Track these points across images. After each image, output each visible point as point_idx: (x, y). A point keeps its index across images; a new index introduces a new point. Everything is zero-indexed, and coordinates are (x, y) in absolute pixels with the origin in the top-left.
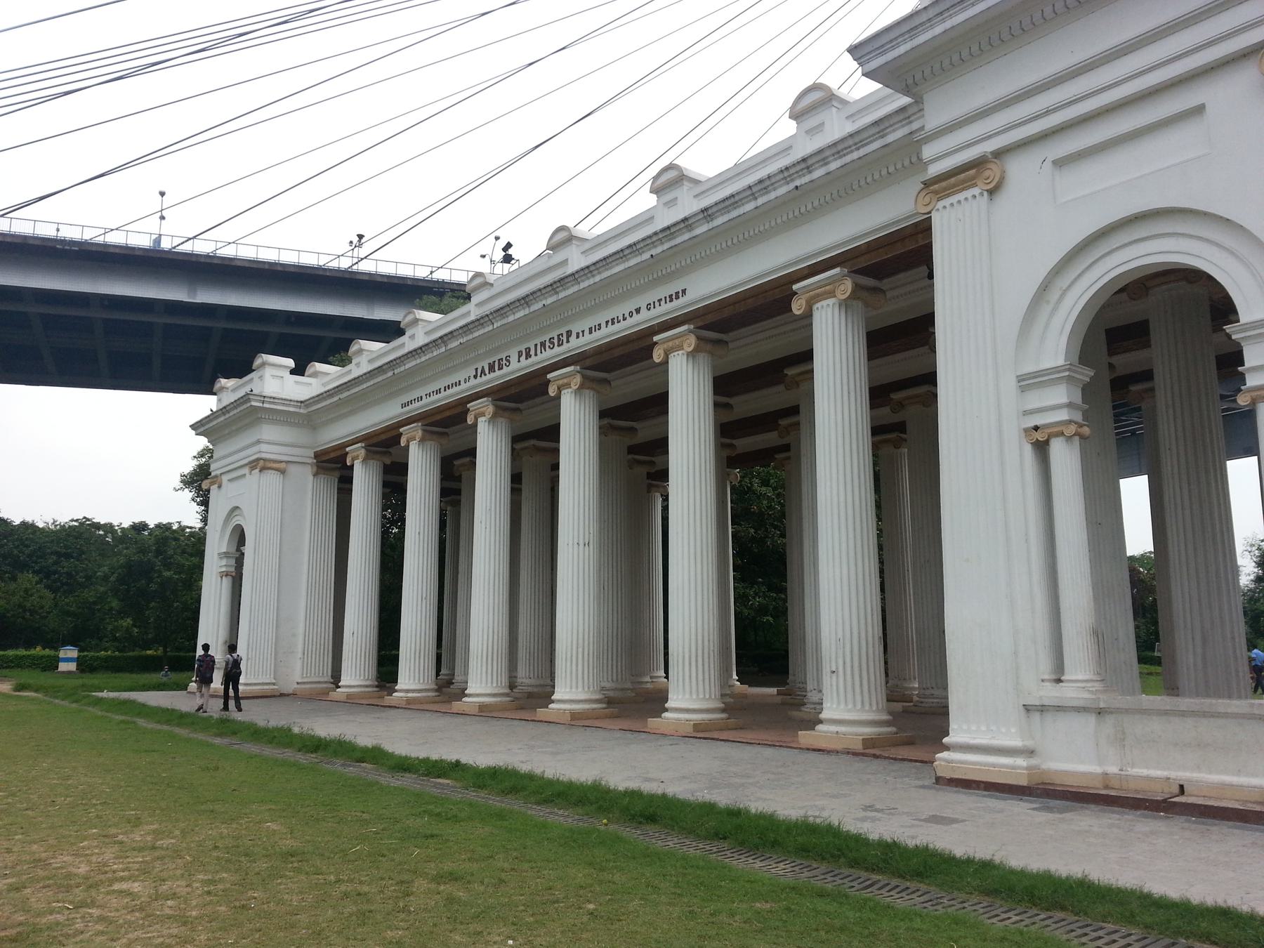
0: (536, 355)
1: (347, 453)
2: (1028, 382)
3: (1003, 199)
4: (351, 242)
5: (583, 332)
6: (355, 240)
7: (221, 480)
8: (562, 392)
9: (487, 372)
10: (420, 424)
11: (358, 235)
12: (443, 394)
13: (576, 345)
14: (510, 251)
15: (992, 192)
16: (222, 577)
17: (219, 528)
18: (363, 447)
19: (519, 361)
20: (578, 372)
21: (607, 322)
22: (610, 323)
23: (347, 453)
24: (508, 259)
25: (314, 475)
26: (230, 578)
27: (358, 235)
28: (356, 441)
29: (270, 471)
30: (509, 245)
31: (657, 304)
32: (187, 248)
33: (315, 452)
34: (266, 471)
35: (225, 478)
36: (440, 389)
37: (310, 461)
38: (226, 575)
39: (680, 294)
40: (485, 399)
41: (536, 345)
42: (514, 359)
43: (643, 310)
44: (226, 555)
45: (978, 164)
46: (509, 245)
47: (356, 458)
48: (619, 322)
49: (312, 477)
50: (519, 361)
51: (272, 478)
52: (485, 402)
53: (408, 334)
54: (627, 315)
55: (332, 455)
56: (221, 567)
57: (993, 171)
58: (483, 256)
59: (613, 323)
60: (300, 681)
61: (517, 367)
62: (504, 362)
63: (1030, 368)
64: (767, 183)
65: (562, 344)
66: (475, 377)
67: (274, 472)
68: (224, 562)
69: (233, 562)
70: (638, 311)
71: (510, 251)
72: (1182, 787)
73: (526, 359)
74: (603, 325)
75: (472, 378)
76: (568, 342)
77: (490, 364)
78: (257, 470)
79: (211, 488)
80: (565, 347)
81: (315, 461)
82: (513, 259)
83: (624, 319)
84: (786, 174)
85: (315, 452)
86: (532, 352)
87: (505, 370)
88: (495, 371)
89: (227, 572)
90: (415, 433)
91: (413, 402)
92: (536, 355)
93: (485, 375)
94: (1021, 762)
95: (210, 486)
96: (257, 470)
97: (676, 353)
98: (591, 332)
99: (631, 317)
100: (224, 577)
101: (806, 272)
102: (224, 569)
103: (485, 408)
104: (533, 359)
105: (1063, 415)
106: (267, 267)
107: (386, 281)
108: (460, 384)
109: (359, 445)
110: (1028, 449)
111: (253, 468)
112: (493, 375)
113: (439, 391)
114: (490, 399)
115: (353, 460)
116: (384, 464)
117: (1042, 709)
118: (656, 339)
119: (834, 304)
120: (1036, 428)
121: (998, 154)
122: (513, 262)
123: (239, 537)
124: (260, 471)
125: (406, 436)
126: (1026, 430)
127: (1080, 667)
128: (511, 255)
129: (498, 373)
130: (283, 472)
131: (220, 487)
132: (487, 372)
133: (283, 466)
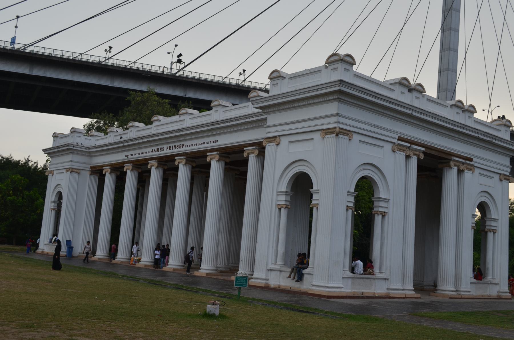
0: (172, 149)
1: (103, 169)
2: (279, 194)
3: (279, 146)
4: (106, 50)
5: (187, 145)
6: (108, 49)
7: (53, 172)
8: (180, 164)
9: (156, 151)
10: (131, 164)
11: (109, 47)
12: (140, 155)
13: (184, 149)
14: (181, 58)
15: (277, 145)
16: (52, 210)
17: (52, 191)
18: (110, 168)
19: (167, 150)
20: (185, 159)
22: (196, 145)
23: (103, 169)
24: (179, 61)
25: (90, 175)
26: (55, 211)
27: (109, 47)
28: (107, 165)
29: (74, 173)
30: (180, 55)
31: (210, 142)
32: (30, 49)
33: (91, 166)
34: (73, 173)
35: (55, 172)
36: (139, 153)
37: (89, 169)
38: (54, 210)
39: (216, 141)
40: (155, 161)
41: (173, 146)
42: (165, 149)
43: (206, 143)
44: (54, 202)
45: (275, 137)
46: (180, 55)
47: (107, 171)
48: (198, 145)
49: (89, 176)
50: (167, 150)
51: (75, 175)
52: (154, 162)
53: (130, 129)
54: (201, 144)
55: (98, 169)
56: (52, 206)
57: (278, 139)
58: (169, 53)
59: (197, 145)
60: (80, 252)
61: (166, 152)
62: (162, 149)
63: (280, 190)
64: (239, 118)
65: (181, 148)
66: (152, 152)
67: (75, 173)
68: (53, 204)
69: (56, 205)
70: (204, 143)
71: (181, 58)
72: (291, 288)
73: (169, 150)
74: (194, 145)
75: (151, 152)
77: (157, 149)
78: (69, 172)
79: (49, 175)
80: (182, 149)
81: (91, 170)
82: (182, 62)
83: (200, 145)
84: (243, 117)
85: (91, 166)
86: (171, 148)
87: (162, 152)
88: (159, 151)
89: (54, 208)
90: (130, 167)
91: (130, 155)
92: (172, 149)
93: (155, 152)
94: (264, 282)
95: (49, 174)
96: (69, 172)
97: (213, 160)
98: (190, 146)
99: (202, 144)
100: (53, 211)
101: (248, 145)
102: (53, 207)
103: (154, 164)
104: (171, 151)
105: (283, 203)
106: (66, 61)
107: (121, 69)
108: (146, 153)
109: (108, 167)
110: (277, 209)
111: (67, 171)
113: (139, 154)
114: (156, 161)
115: (106, 172)
116: (117, 175)
117: (271, 270)
118: (208, 154)
119: (254, 156)
120: (279, 205)
121: (279, 136)
122: (182, 63)
123: (60, 196)
124: (70, 173)
125: (126, 167)
126: (277, 205)
127: (280, 262)
128: (181, 60)
129: (160, 153)
130: (79, 173)
131: (53, 175)
132: (156, 151)
133: (79, 171)
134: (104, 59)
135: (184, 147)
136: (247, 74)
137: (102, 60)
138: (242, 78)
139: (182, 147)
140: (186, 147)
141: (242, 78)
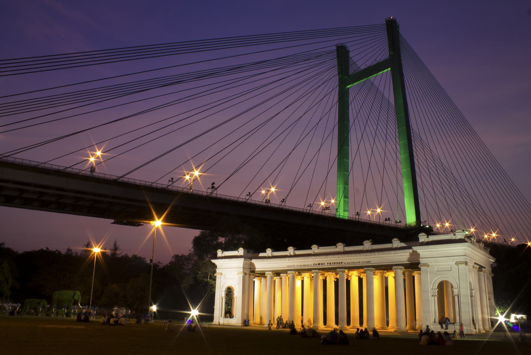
14: (214, 185)
24: (213, 187)
30: (213, 183)
42: (326, 264)
46: (213, 183)
66: (314, 265)
71: (214, 185)
74: (351, 263)
76: (342, 264)
80: (341, 264)
92: (333, 264)
93: (317, 265)
112: (319, 266)
134: (167, 186)
135: (343, 264)
136: (251, 194)
137: (165, 187)
138: (248, 197)
139: (341, 263)
140: (344, 263)
141: (248, 197)
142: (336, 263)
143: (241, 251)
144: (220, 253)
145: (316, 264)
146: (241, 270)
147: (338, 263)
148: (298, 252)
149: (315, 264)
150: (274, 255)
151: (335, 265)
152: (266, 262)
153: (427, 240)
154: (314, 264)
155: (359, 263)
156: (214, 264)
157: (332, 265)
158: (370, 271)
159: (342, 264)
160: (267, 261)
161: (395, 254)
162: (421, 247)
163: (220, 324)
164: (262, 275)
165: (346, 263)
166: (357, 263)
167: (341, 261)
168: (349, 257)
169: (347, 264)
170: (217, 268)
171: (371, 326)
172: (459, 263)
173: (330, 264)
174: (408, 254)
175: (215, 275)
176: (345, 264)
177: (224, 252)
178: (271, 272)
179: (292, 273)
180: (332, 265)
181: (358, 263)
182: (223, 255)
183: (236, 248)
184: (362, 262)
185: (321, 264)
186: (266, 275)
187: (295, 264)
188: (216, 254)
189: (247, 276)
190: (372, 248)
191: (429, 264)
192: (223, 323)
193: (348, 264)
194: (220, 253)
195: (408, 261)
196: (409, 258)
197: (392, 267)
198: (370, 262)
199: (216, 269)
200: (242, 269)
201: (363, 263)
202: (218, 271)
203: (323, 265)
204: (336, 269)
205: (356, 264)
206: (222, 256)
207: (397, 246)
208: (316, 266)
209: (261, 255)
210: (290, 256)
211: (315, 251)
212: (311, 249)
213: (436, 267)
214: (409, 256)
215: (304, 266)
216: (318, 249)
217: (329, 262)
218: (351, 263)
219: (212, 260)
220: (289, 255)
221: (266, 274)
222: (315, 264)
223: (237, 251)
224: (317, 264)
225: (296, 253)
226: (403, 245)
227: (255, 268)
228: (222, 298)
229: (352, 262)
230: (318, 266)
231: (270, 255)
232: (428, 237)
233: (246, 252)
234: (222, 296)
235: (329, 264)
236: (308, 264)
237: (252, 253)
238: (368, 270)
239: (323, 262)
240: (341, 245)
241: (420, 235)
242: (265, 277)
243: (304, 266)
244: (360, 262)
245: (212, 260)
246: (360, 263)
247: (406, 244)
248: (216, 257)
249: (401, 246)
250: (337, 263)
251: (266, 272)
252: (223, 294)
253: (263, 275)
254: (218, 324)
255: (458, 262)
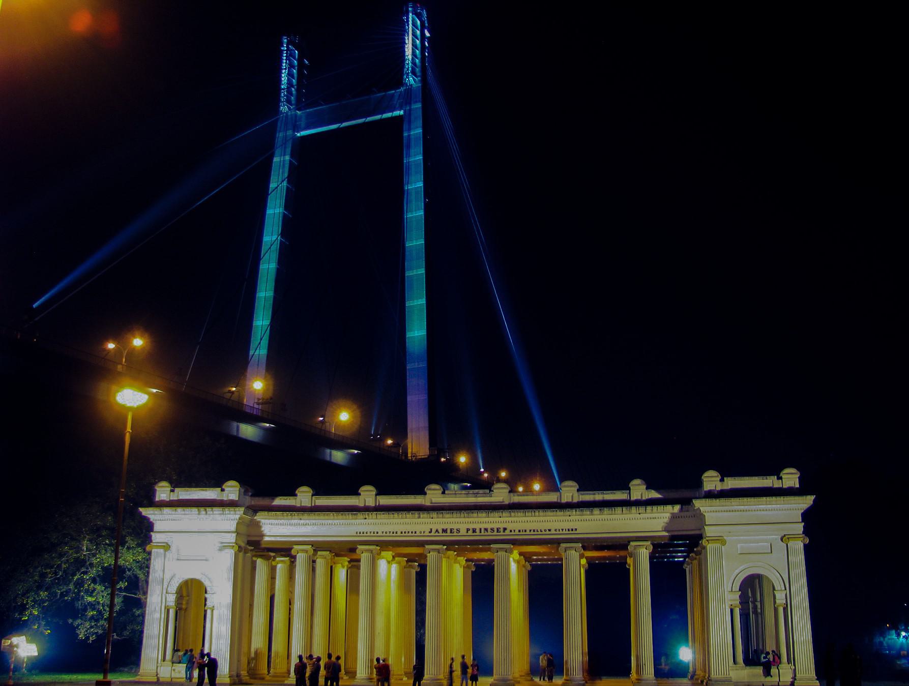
0: (481, 532)
19: (467, 532)
21: (530, 531)
42: (463, 532)
50: (467, 532)
73: (473, 532)
74: (528, 531)
76: (504, 532)
92: (481, 532)
93: (438, 533)
112: (444, 534)
135: (507, 532)
140: (511, 531)
142: (489, 530)
143: (232, 490)
144: (163, 492)
145: (437, 531)
146: (232, 538)
147: (495, 530)
148: (385, 500)
149: (434, 531)
150: (316, 504)
151: (486, 534)
152: (363, 521)
153: (719, 487)
154: (431, 529)
155: (548, 532)
156: (146, 519)
157: (478, 533)
158: (505, 553)
159: (504, 532)
160: (568, 513)
161: (640, 514)
162: (708, 501)
163: (161, 680)
164: (285, 550)
165: (514, 531)
166: (544, 533)
167: (502, 526)
168: (481, 517)
169: (517, 532)
170: (156, 528)
171: (649, 676)
172: (788, 538)
173: (474, 531)
174: (668, 515)
175: (148, 548)
176: (513, 533)
177: (177, 490)
178: (311, 546)
179: (371, 551)
180: (478, 533)
181: (545, 531)
182: (174, 497)
183: (218, 483)
184: (556, 530)
185: (449, 531)
186: (293, 552)
187: (380, 529)
188: (154, 492)
189: (241, 554)
190: (512, 502)
191: (725, 538)
192: (169, 676)
193: (574, 532)
194: (163, 492)
195: (666, 530)
196: (667, 523)
197: (629, 542)
198: (576, 530)
199: (152, 533)
200: (234, 535)
201: (558, 532)
202: (156, 537)
203: (455, 534)
204: (559, 543)
205: (540, 533)
206: (171, 499)
207: (570, 500)
208: (437, 534)
209: (279, 501)
210: (366, 509)
211: (434, 500)
212: (425, 494)
213: (739, 546)
214: (666, 520)
215: (403, 534)
216: (444, 495)
217: (471, 526)
218: (528, 531)
219: (141, 509)
220: (362, 505)
221: (357, 551)
222: (434, 531)
223: (220, 489)
224: (440, 531)
225: (380, 500)
226: (654, 495)
227: (263, 535)
228: (168, 611)
229: (532, 529)
230: (441, 534)
231: (371, 502)
232: (722, 480)
233: (243, 490)
234: (167, 604)
235: (470, 533)
236: (524, 529)
237: (251, 496)
238: (571, 548)
239: (455, 527)
240: (504, 488)
241: (707, 474)
242: (293, 559)
243: (571, 532)
244: (550, 530)
245: (141, 509)
246: (550, 533)
247: (660, 493)
248: (151, 502)
249: (650, 497)
250: (492, 530)
251: (295, 546)
252: (172, 599)
253: (261, 553)
254: (156, 680)
255: (787, 536)
